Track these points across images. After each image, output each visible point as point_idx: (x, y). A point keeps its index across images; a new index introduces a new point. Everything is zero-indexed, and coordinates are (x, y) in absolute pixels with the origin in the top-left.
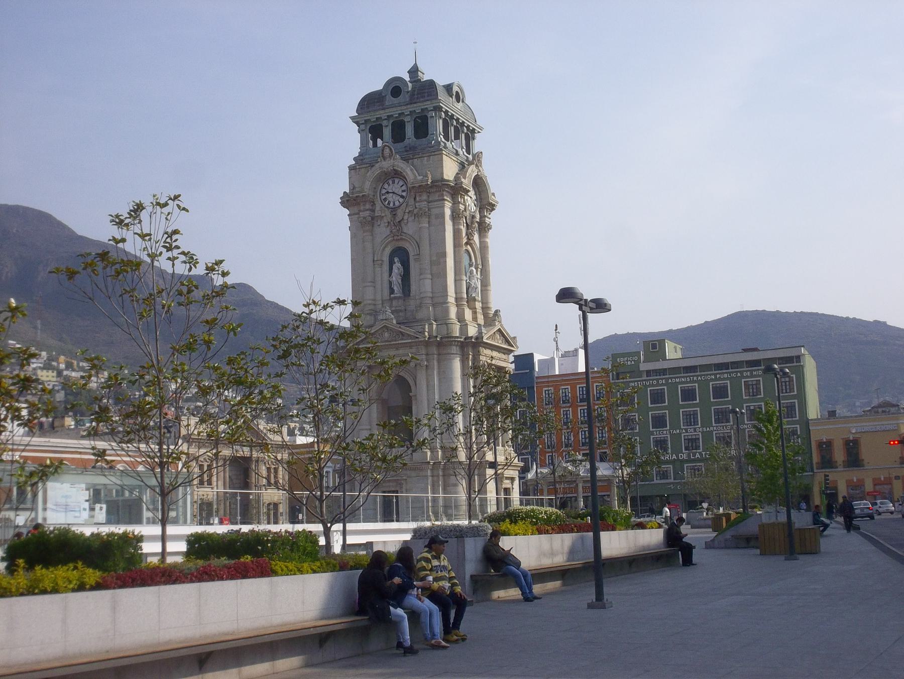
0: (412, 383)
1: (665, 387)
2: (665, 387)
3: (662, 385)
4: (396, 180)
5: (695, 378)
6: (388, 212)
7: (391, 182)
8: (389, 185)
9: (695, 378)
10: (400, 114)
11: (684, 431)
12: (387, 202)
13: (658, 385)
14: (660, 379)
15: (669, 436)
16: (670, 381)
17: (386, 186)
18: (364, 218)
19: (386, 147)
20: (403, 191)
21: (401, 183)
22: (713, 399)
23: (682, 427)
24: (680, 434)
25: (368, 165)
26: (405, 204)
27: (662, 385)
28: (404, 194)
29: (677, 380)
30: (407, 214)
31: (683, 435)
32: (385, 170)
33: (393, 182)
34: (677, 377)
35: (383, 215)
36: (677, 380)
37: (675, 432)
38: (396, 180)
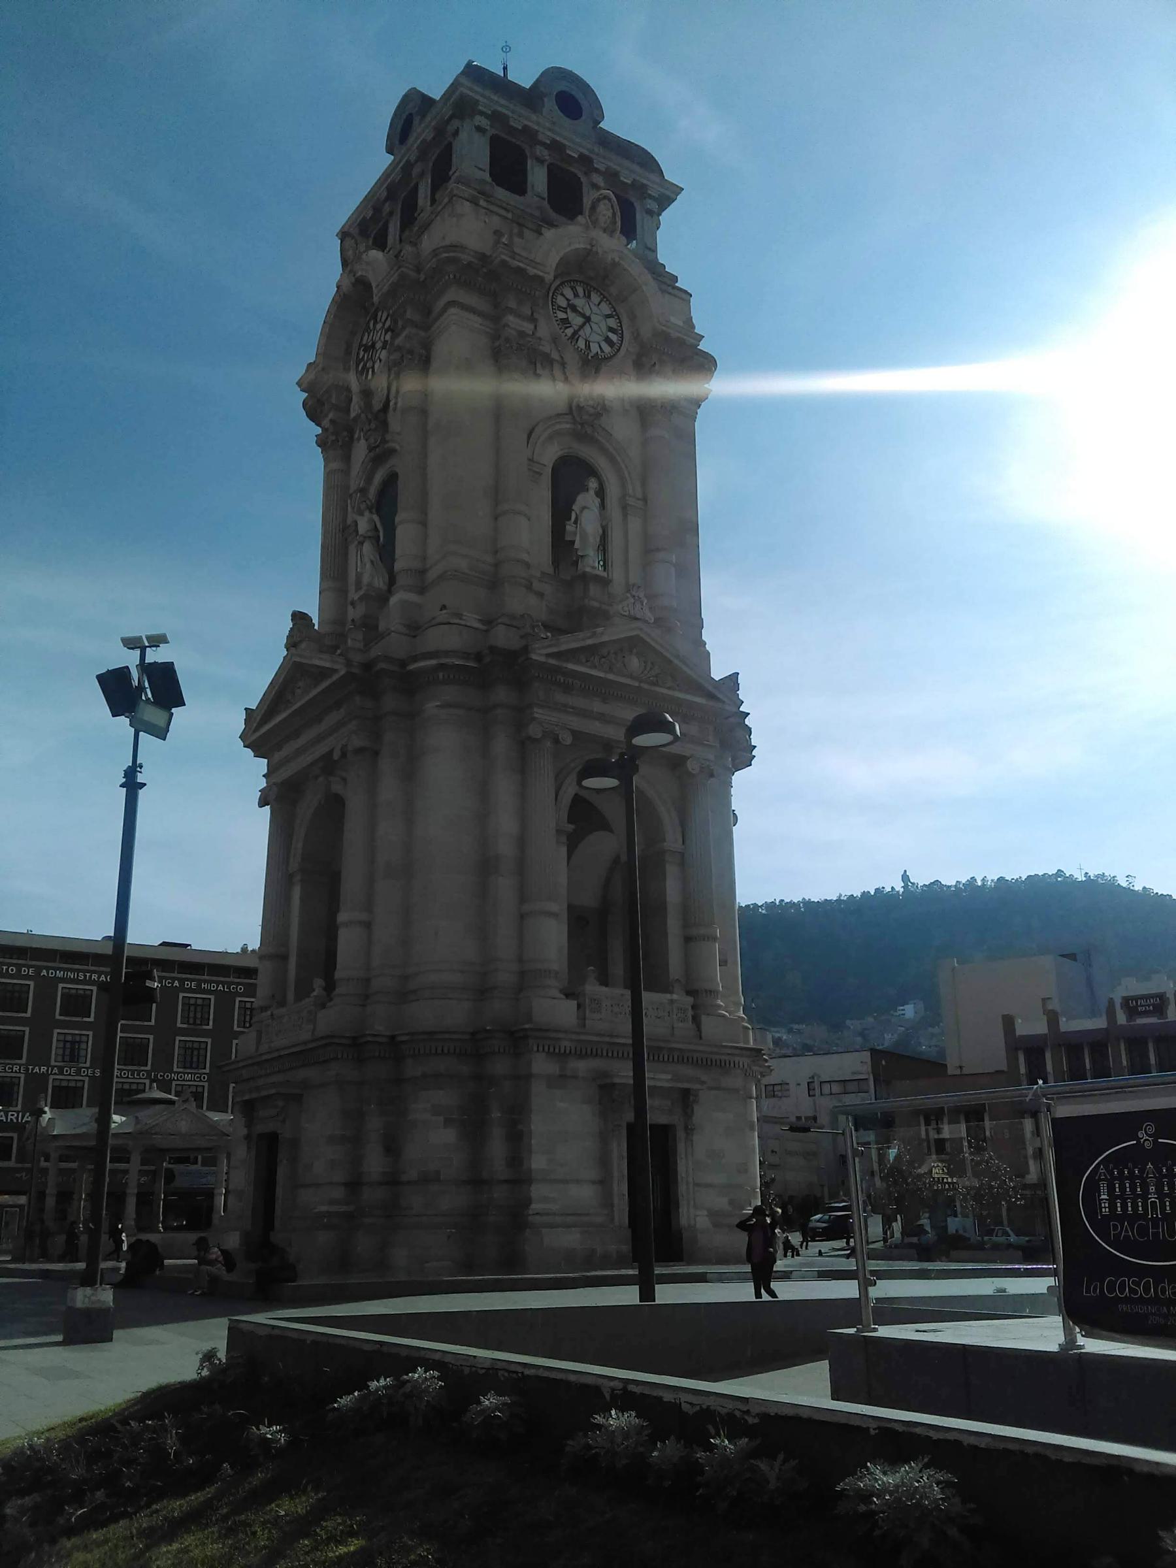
1: (32, 983)
2: (32, 983)
3: (27, 977)
5: (95, 977)
7: (580, 290)
9: (95, 977)
11: (56, 1070)
13: (18, 975)
14: (24, 966)
15: (22, 1076)
16: (44, 972)
19: (606, 201)
21: (606, 309)
22: (60, 1015)
23: (53, 1063)
24: (45, 1076)
27: (27, 977)
29: (60, 974)
31: (52, 1077)
32: (600, 251)
34: (60, 969)
36: (60, 974)
37: (37, 1070)
38: (595, 298)
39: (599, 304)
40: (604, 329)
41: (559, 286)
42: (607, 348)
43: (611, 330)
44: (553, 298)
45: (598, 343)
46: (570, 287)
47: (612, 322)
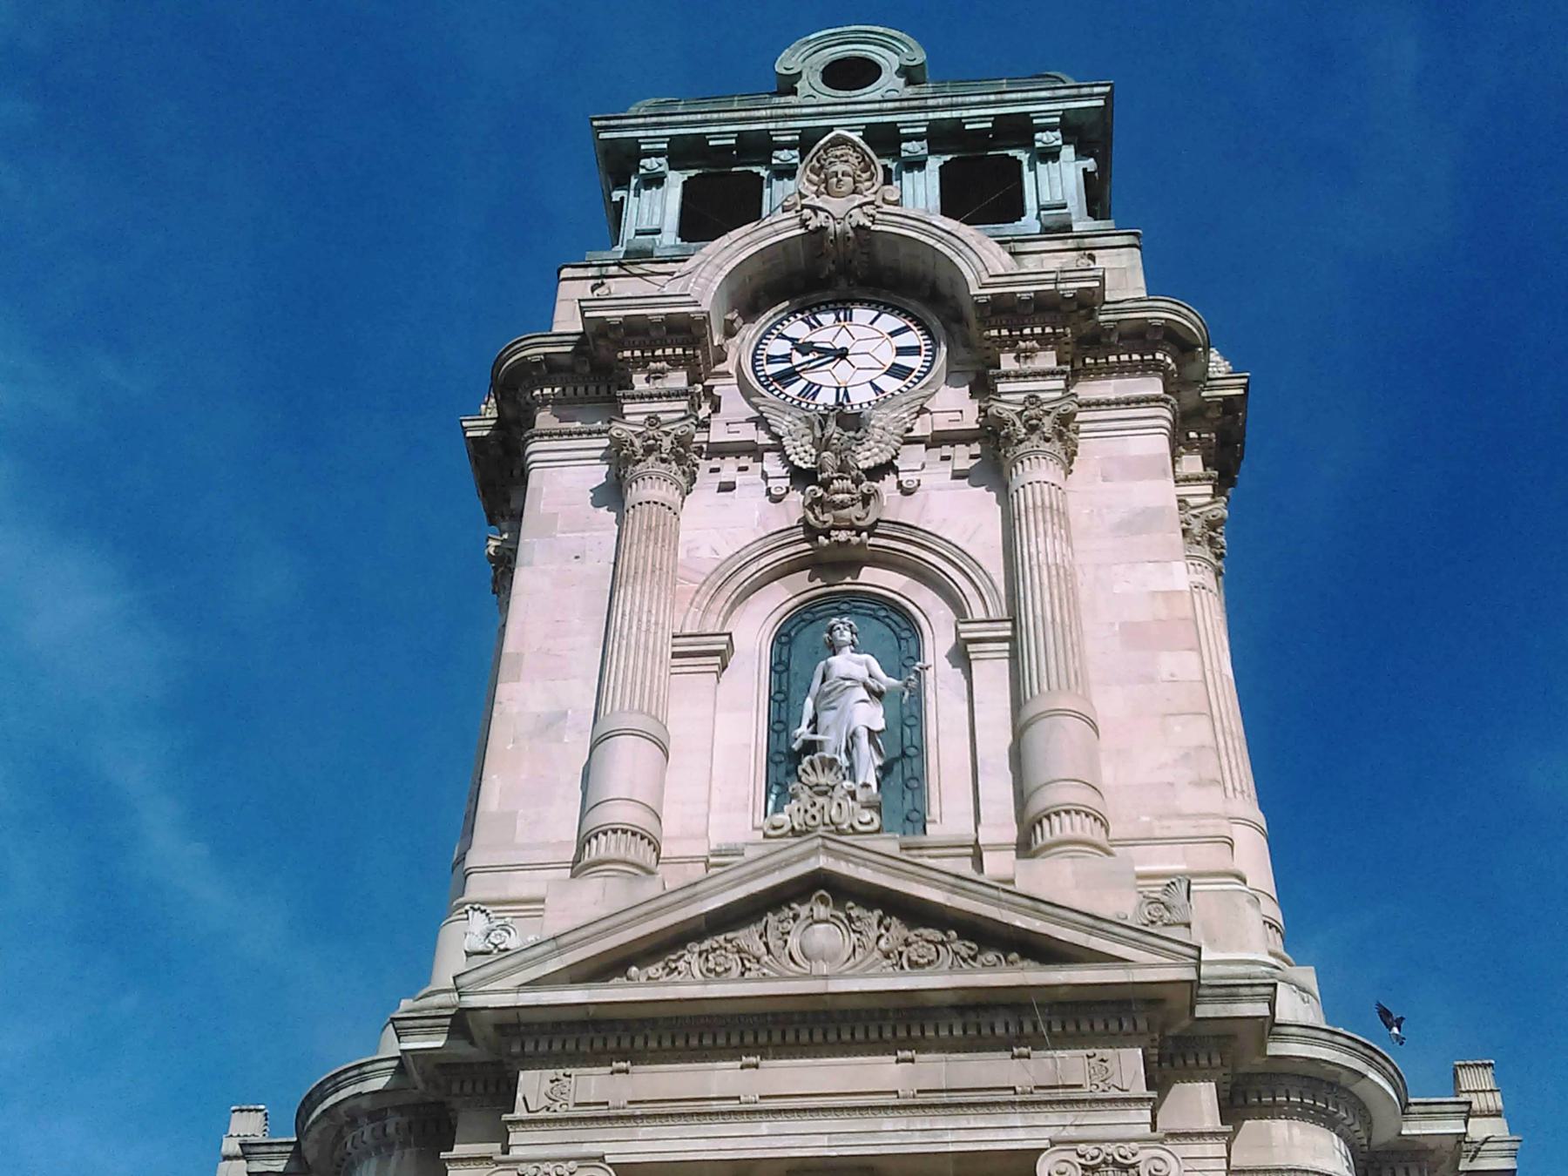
28: (914, 362)
35: (763, 438)
39: (872, 323)
42: (891, 385)
43: (901, 351)
45: (871, 382)
46: (802, 319)
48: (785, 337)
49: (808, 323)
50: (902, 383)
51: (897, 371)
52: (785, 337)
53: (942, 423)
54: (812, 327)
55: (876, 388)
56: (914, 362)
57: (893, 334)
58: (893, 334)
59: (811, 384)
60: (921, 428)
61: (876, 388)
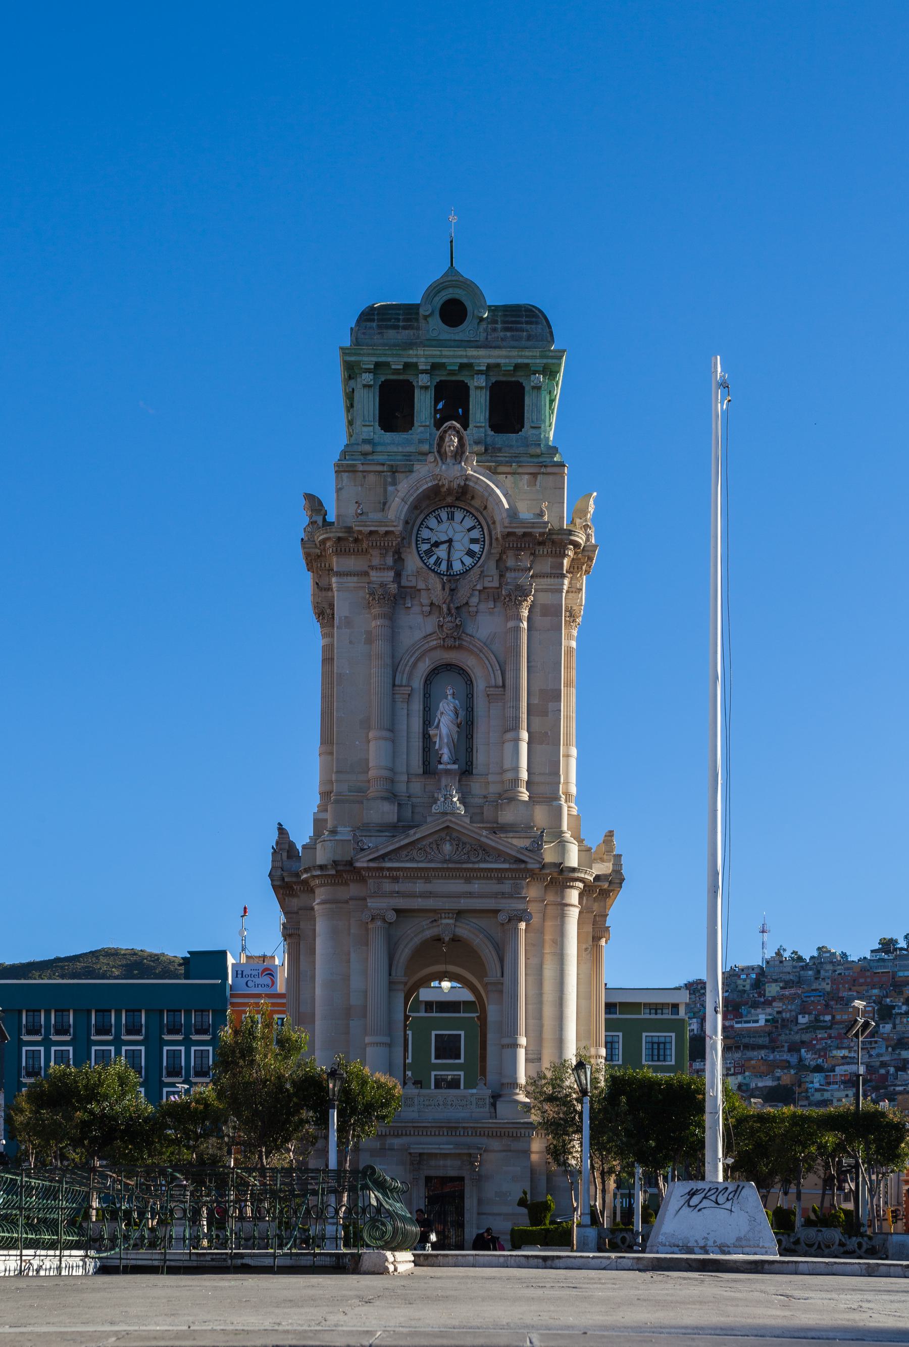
0: (488, 954)
4: (458, 515)
6: (435, 583)
7: (444, 515)
8: (440, 521)
10: (463, 366)
12: (432, 560)
17: (432, 522)
18: (383, 585)
20: (474, 541)
21: (469, 522)
25: (385, 468)
26: (476, 570)
28: (476, 548)
30: (477, 593)
33: (451, 518)
35: (421, 585)
38: (458, 515)
39: (461, 522)
40: (466, 540)
41: (423, 520)
42: (468, 561)
43: (474, 541)
44: (418, 530)
47: (475, 534)
48: (428, 527)
49: (437, 519)
50: (472, 560)
51: (470, 553)
52: (428, 527)
53: (487, 584)
54: (438, 521)
55: (462, 562)
56: (476, 548)
57: (469, 530)
58: (469, 530)
59: (438, 558)
60: (479, 587)
61: (462, 562)
